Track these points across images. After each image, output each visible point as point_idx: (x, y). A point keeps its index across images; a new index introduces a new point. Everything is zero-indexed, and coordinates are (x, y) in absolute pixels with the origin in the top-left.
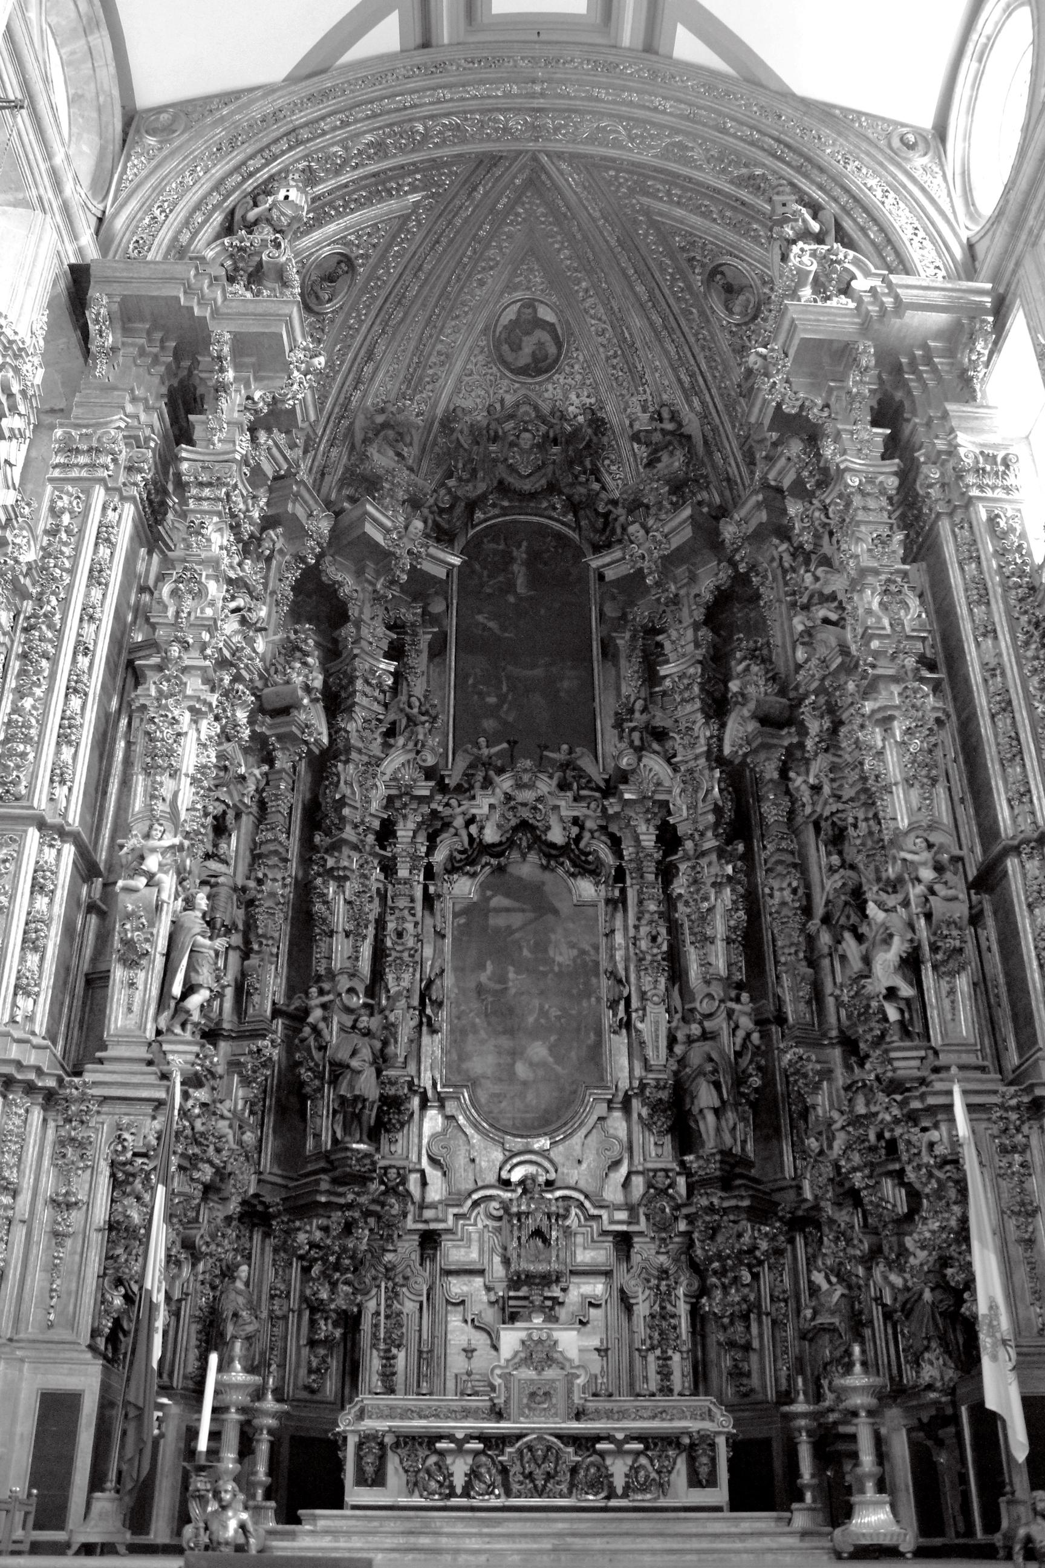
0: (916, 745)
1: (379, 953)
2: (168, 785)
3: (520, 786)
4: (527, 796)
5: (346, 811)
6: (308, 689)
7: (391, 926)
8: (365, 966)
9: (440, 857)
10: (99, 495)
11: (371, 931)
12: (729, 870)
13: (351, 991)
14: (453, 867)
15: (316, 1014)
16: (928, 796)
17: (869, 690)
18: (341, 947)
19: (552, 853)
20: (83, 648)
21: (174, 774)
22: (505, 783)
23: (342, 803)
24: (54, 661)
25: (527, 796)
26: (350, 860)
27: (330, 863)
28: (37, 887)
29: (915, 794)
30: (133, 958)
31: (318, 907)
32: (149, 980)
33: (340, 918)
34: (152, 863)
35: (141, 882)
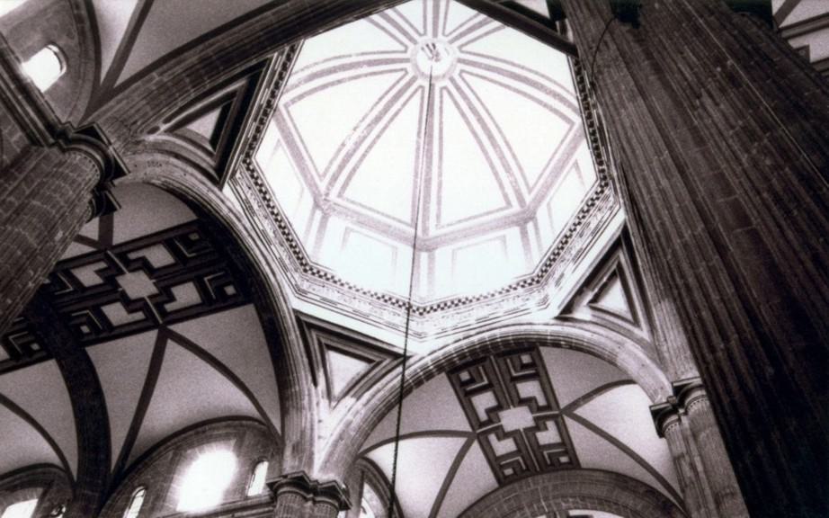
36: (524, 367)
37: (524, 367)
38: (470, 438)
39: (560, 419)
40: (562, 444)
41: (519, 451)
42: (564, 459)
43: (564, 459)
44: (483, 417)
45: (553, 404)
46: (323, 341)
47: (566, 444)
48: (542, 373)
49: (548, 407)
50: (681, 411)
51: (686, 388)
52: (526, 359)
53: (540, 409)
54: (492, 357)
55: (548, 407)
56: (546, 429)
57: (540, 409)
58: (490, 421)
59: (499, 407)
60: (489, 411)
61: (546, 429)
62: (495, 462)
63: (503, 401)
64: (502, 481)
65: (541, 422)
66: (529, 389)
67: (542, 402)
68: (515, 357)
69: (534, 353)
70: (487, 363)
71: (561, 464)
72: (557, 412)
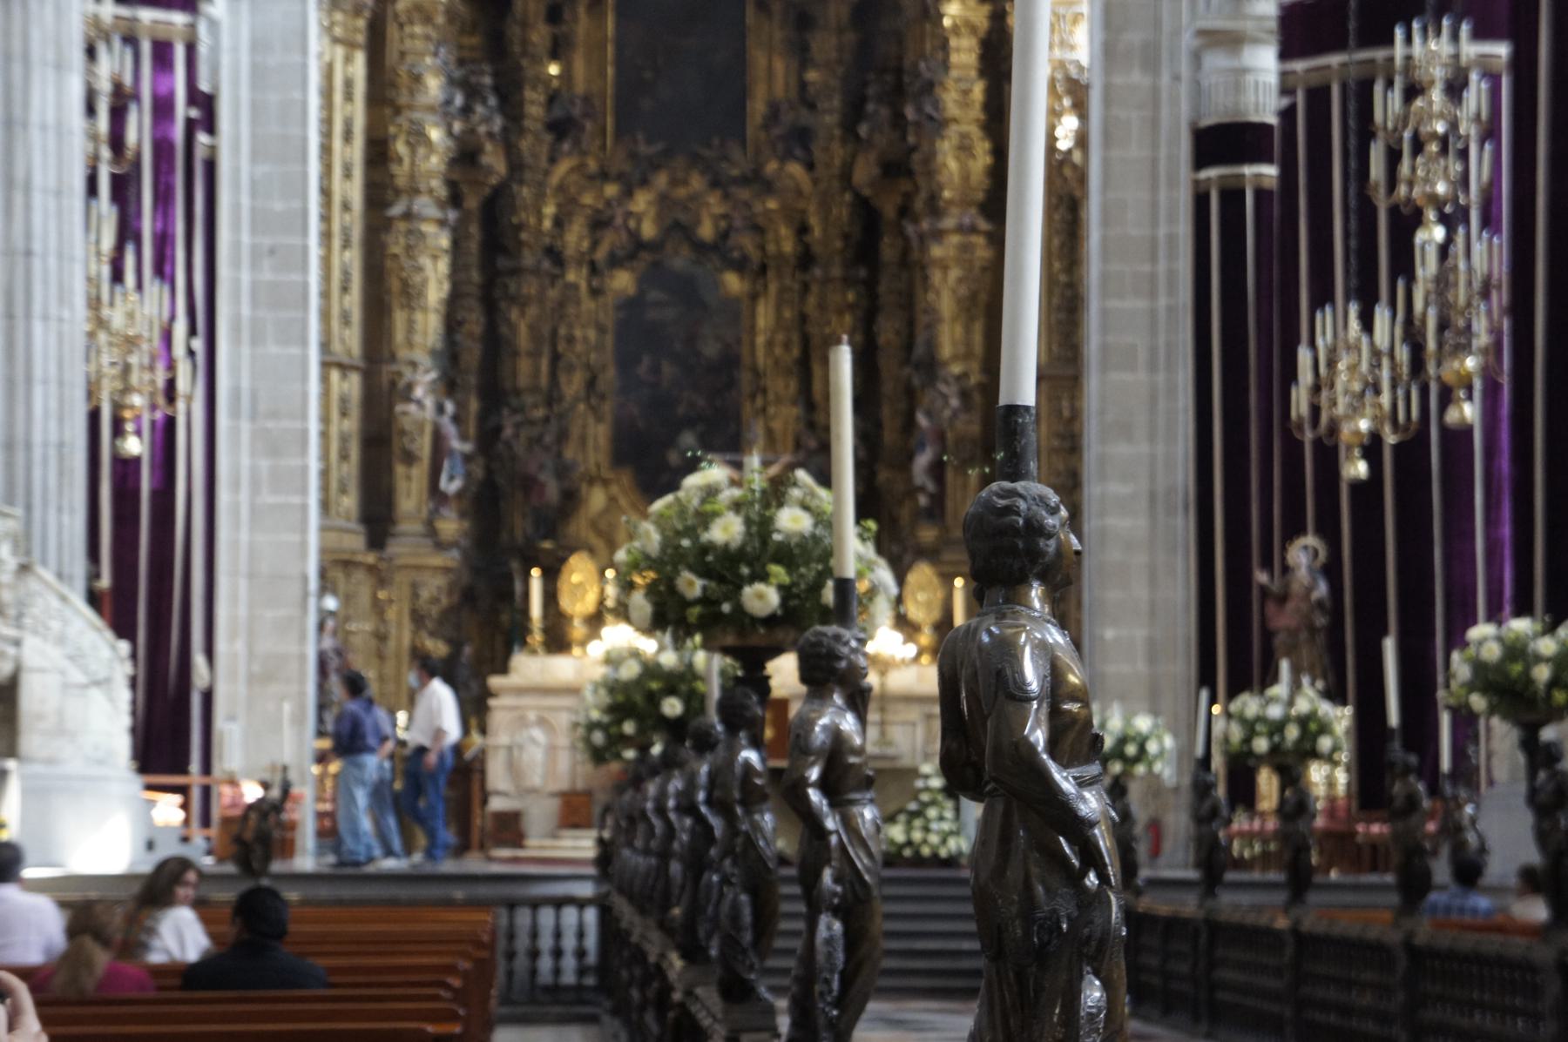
0: (963, 291)
1: (556, 358)
2: (419, 316)
3: (674, 182)
4: (681, 192)
5: (524, 236)
6: (490, 135)
7: (562, 331)
8: (544, 381)
9: (601, 254)
11: (546, 350)
12: (851, 297)
13: (535, 406)
14: (615, 262)
15: (508, 432)
16: (968, 330)
17: (939, 235)
18: (524, 366)
19: (700, 247)
20: (346, 207)
21: (425, 309)
22: (661, 180)
23: (520, 227)
25: (681, 192)
26: (530, 287)
27: (513, 287)
28: (344, 414)
29: (959, 330)
30: (410, 458)
31: (504, 330)
32: (420, 472)
33: (523, 339)
34: (419, 392)
35: (412, 408)
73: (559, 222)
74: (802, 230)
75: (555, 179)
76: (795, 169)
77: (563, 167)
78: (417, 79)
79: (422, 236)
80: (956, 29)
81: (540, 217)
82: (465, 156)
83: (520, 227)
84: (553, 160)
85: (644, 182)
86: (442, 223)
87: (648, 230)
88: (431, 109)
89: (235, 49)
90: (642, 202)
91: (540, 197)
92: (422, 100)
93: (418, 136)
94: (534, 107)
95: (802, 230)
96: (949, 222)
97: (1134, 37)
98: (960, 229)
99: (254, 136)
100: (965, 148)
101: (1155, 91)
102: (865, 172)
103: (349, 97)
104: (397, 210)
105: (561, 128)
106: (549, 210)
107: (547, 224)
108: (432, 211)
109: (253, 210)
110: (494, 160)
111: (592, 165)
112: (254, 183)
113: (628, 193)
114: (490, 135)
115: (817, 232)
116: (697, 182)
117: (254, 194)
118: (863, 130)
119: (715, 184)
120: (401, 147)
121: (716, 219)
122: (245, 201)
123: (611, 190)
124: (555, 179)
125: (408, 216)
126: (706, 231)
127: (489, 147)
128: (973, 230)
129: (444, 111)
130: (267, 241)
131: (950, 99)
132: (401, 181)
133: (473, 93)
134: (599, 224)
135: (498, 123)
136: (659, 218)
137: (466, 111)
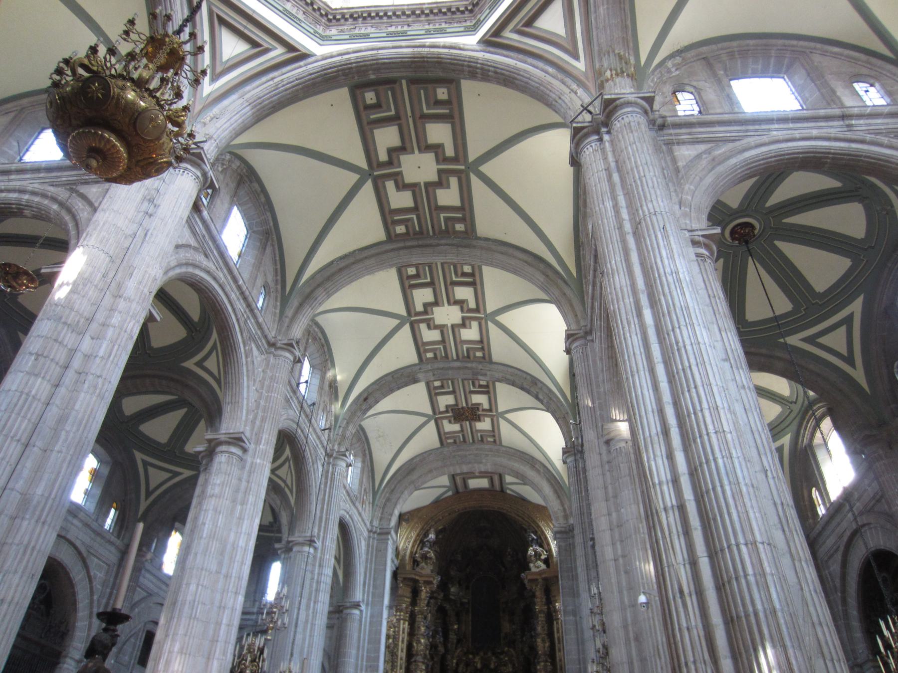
6: (440, 642)
10: (402, 622)
17: (539, 663)
20: (401, 659)
22: (482, 654)
23: (447, 665)
24: (397, 662)
36: (438, 103)
37: (438, 103)
38: (364, 176)
39: (463, 176)
40: (461, 209)
41: (415, 209)
42: (460, 227)
43: (460, 227)
44: (383, 157)
45: (462, 159)
46: (215, 10)
47: (466, 209)
48: (457, 116)
49: (455, 160)
50: (604, 130)
51: (618, 102)
52: (442, 93)
53: (446, 160)
54: (404, 82)
55: (455, 160)
56: (448, 187)
57: (446, 160)
58: (390, 163)
59: (403, 149)
60: (391, 151)
61: (448, 187)
62: (388, 215)
63: (408, 145)
64: (391, 237)
65: (444, 176)
66: (439, 133)
67: (450, 152)
68: (430, 86)
69: (453, 86)
70: (397, 86)
71: (455, 232)
72: (463, 167)
73: (457, 664)
74: (514, 665)
75: (456, 654)
76: (511, 650)
77: (459, 651)
78: (419, 627)
79: (418, 665)
80: (540, 612)
81: (452, 663)
82: (433, 647)
83: (447, 665)
84: (456, 649)
85: (478, 654)
86: (423, 663)
87: (479, 666)
88: (422, 635)
89: (366, 618)
90: (477, 659)
91: (453, 658)
92: (420, 633)
93: (419, 642)
94: (453, 637)
95: (514, 665)
96: (541, 660)
97: (570, 608)
98: (543, 661)
99: (369, 640)
100: (543, 641)
101: (576, 620)
102: (526, 650)
103: (403, 632)
104: (413, 660)
105: (459, 641)
106: (455, 661)
107: (454, 665)
108: (421, 660)
109: (367, 656)
110: (441, 649)
111: (465, 650)
112: (368, 649)
113: (474, 658)
114: (440, 642)
115: (516, 665)
116: (490, 654)
117: (367, 653)
118: (524, 639)
119: (494, 654)
120: (415, 644)
121: (495, 663)
122: (365, 654)
123: (471, 656)
124: (456, 654)
125: (415, 661)
126: (492, 666)
127: (440, 645)
128: (546, 661)
129: (427, 637)
130: (369, 664)
131: (539, 629)
132: (414, 652)
133: (435, 632)
134: (467, 665)
135: (442, 639)
136: (481, 663)
137: (433, 637)
